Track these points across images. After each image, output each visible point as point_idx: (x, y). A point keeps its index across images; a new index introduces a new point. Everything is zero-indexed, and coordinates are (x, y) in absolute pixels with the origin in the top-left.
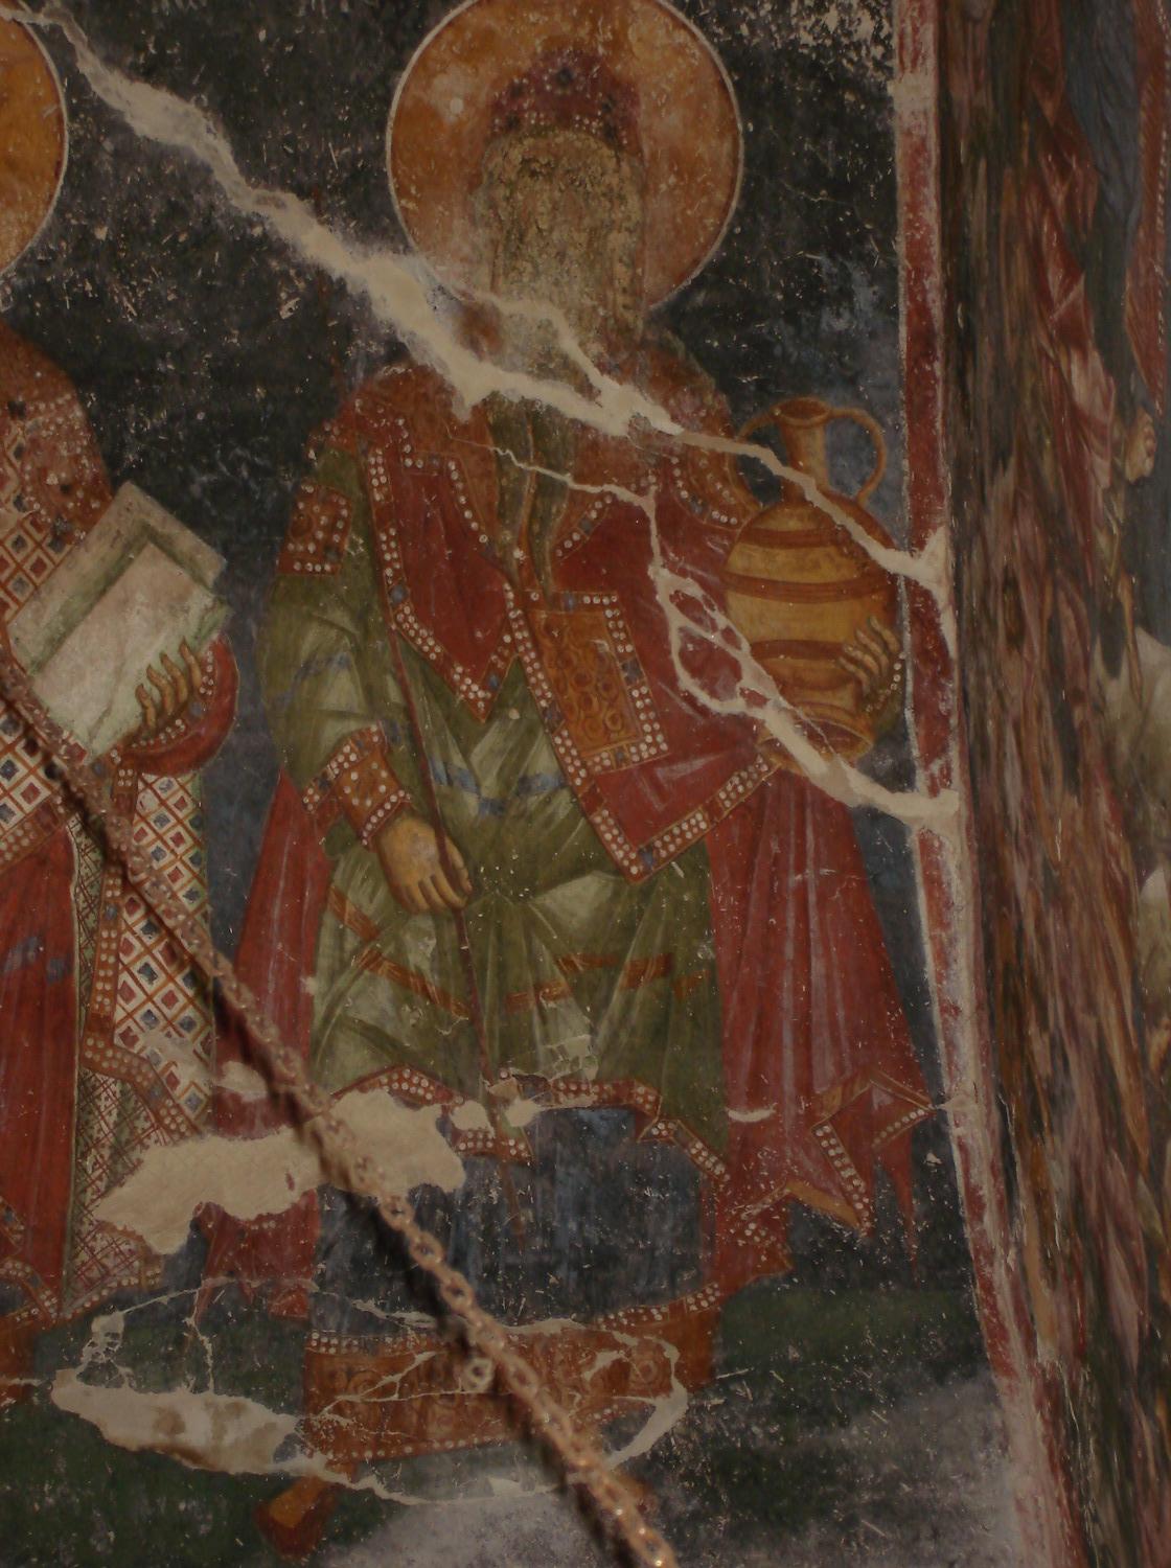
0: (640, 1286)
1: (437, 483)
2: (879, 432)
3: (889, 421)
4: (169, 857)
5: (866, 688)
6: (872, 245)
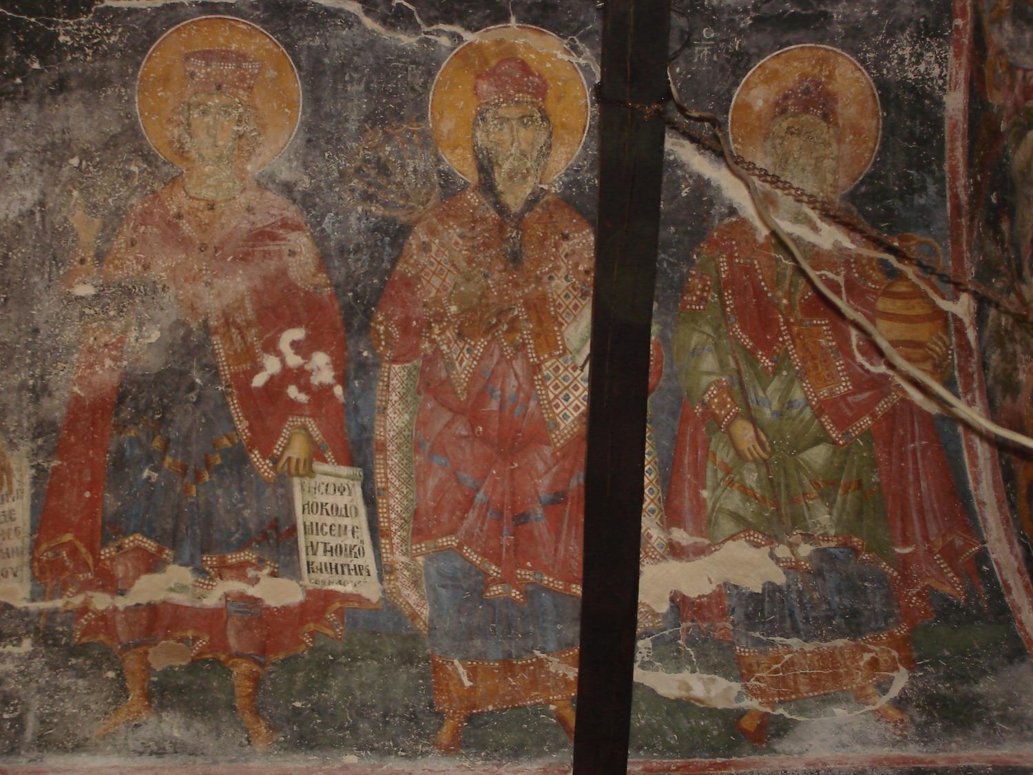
0: (873, 625)
1: (749, 270)
2: (939, 249)
3: (943, 244)
5: (937, 362)
6: (934, 167)
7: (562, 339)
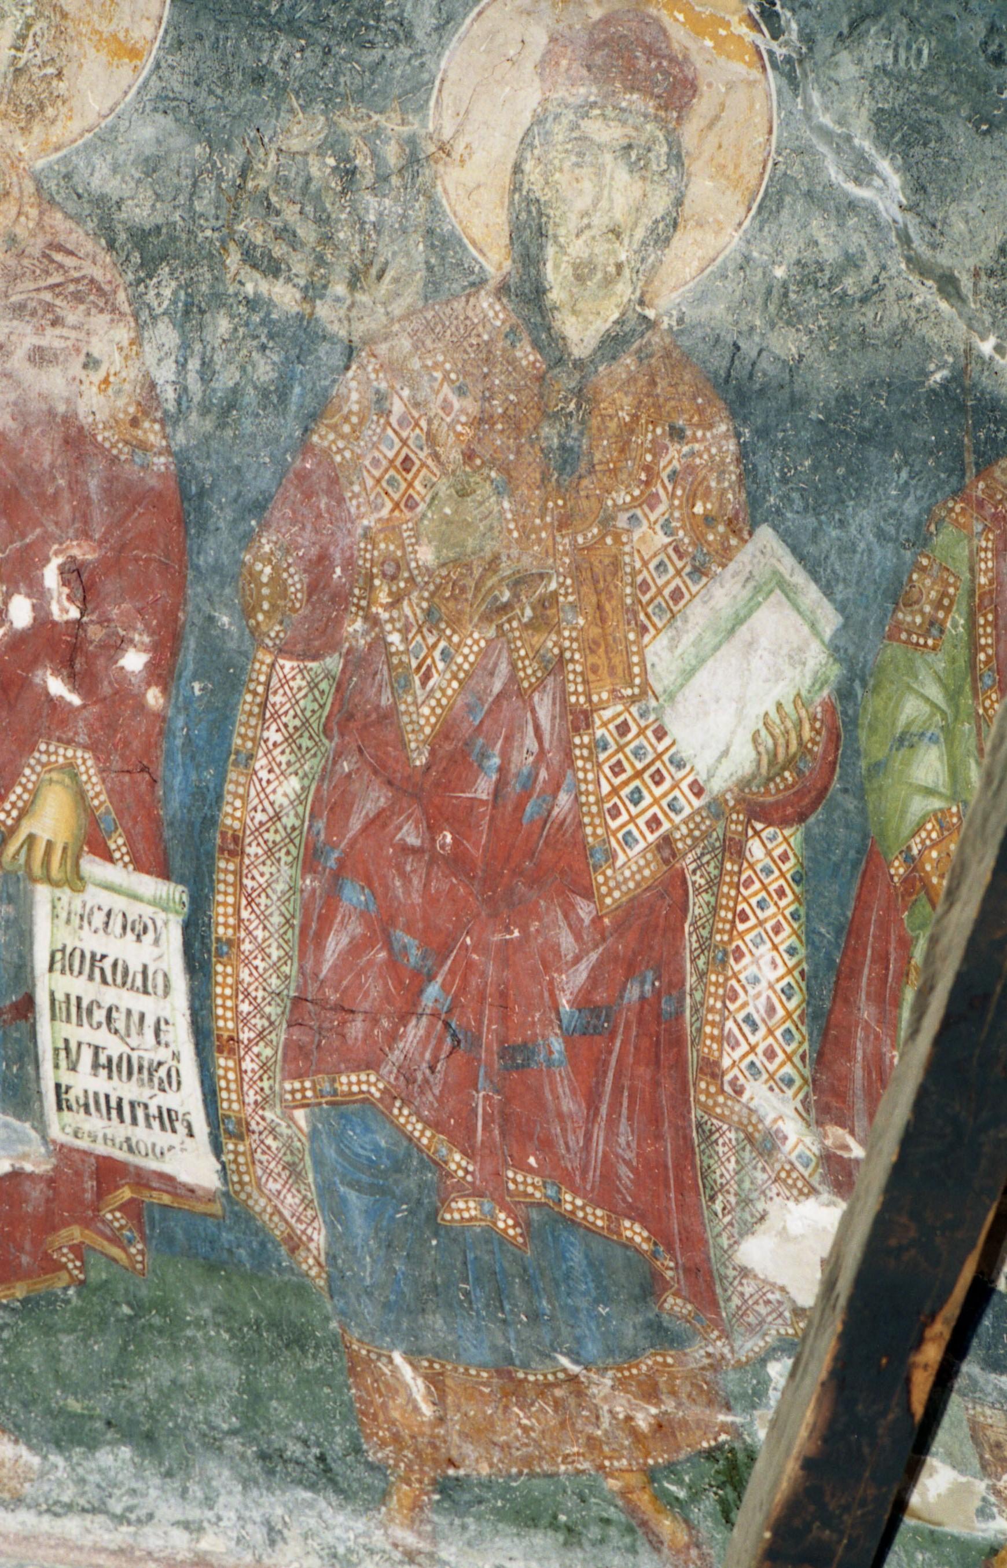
4: (773, 909)
7: (643, 663)
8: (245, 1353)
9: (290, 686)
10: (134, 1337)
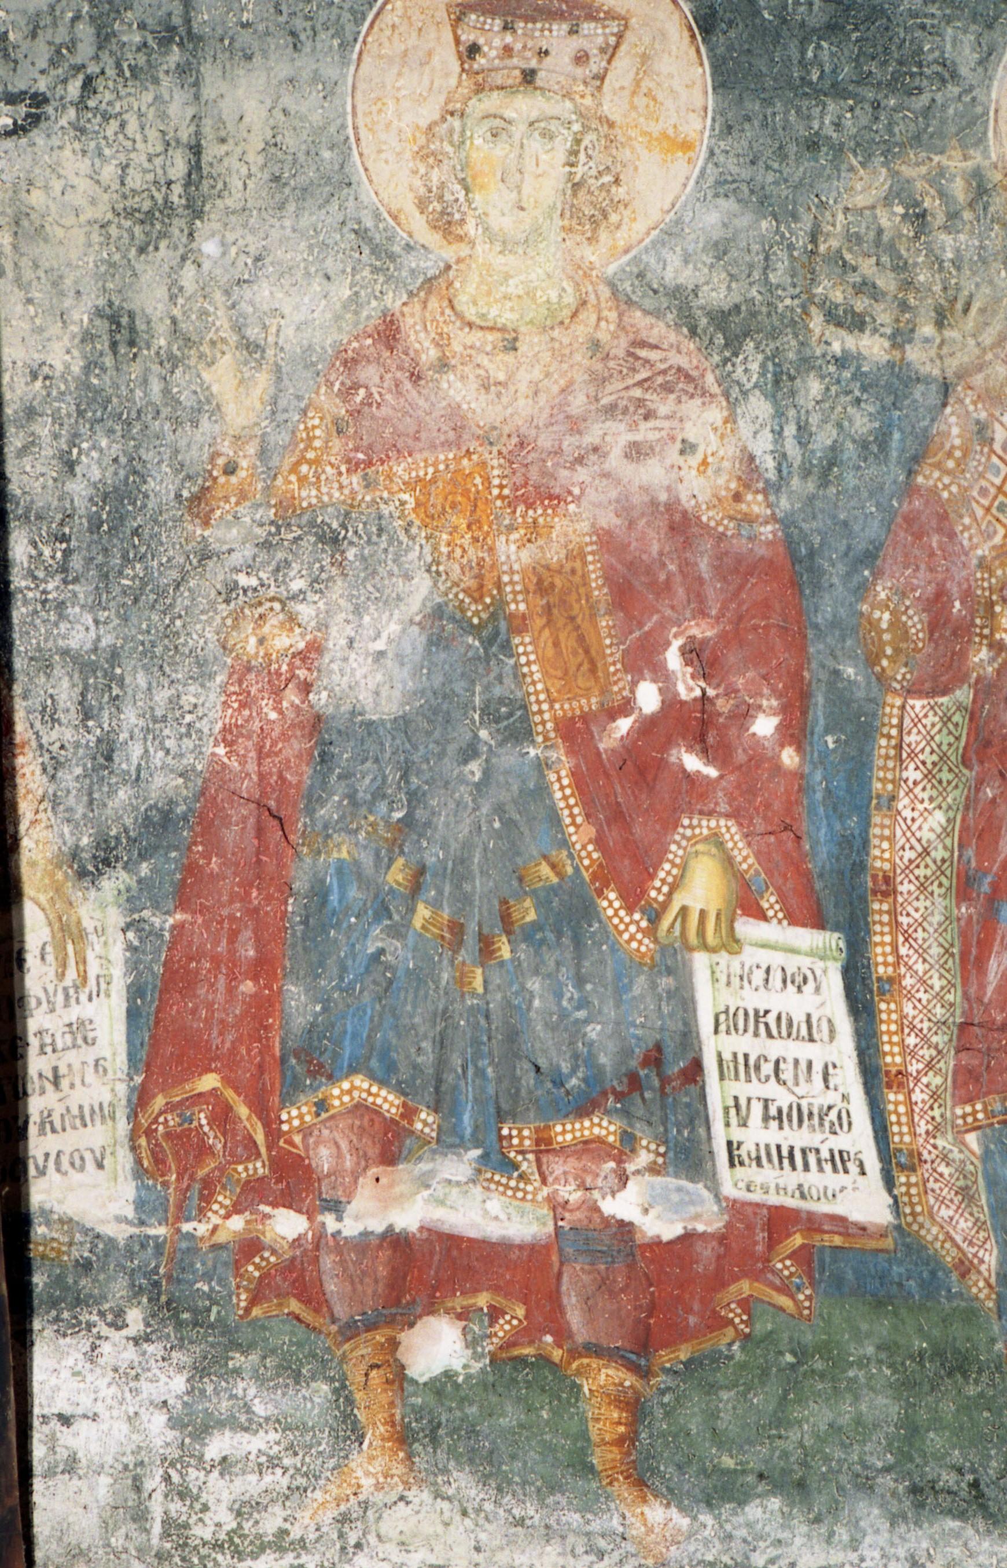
8: (906, 1386)
9: (923, 724)
10: (794, 1385)
